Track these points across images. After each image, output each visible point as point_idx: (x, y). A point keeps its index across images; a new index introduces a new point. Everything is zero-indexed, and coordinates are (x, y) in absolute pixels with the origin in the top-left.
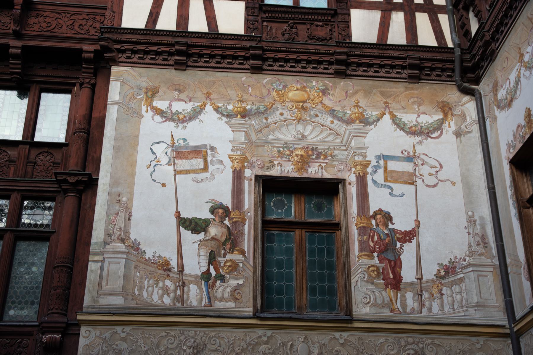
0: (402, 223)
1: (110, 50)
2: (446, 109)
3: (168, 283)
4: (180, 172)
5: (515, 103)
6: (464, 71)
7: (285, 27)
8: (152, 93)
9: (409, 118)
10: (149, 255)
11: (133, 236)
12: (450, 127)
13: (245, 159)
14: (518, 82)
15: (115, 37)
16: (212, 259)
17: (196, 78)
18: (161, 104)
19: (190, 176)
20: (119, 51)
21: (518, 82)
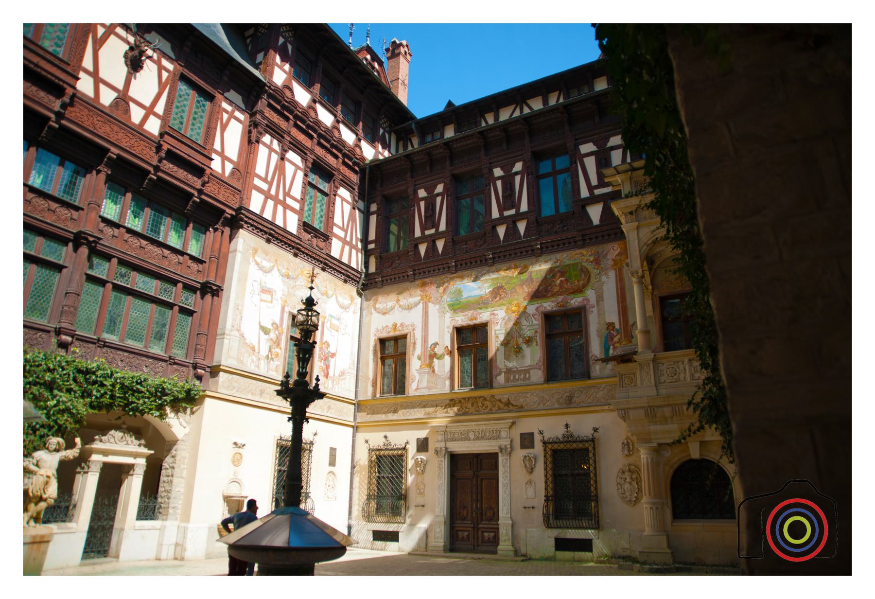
0: (332, 349)
1: (242, 220)
2: (352, 299)
3: (253, 357)
4: (262, 300)
5: (387, 316)
6: (363, 284)
7: (309, 236)
8: (255, 251)
9: (341, 299)
10: (247, 341)
11: (242, 329)
12: (352, 308)
13: (286, 301)
14: (392, 308)
15: (247, 214)
16: (270, 351)
17: (273, 248)
18: (258, 259)
19: (265, 304)
20: (246, 223)
21: (392, 308)
